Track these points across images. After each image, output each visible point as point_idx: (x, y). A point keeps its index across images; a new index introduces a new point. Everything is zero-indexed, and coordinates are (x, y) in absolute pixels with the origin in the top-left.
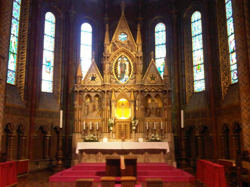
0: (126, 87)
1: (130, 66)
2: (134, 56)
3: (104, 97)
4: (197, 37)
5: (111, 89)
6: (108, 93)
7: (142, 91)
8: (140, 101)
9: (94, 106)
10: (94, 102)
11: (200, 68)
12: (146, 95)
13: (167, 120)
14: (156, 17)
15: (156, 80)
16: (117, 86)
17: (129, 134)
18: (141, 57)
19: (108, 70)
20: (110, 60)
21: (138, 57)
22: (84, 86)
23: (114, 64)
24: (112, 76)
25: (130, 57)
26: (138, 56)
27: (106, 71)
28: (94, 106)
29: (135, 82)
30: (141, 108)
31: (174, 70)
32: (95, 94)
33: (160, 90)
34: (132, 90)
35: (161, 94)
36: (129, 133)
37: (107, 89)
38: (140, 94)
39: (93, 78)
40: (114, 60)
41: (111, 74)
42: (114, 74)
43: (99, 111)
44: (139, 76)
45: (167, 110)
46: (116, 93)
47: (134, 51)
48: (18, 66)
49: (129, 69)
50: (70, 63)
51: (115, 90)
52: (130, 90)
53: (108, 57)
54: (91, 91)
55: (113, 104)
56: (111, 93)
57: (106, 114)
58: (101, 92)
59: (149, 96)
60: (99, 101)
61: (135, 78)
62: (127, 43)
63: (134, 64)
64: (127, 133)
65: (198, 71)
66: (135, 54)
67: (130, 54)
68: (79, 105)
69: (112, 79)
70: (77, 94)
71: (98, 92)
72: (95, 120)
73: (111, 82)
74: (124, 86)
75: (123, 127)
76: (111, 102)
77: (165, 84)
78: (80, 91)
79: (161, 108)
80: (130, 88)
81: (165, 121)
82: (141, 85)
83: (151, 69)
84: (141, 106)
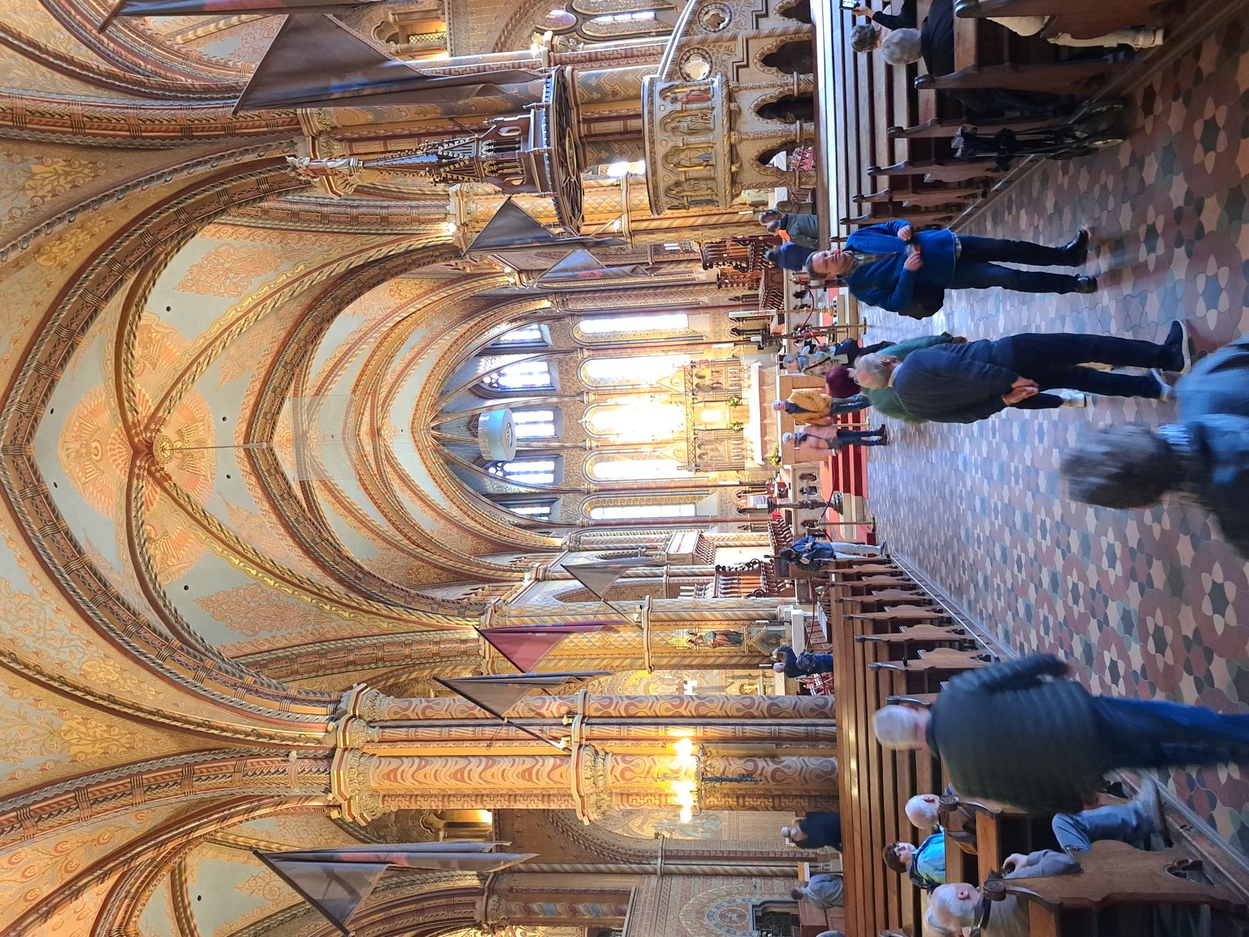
35: (695, 371)
50: (654, 486)
55: (709, 428)
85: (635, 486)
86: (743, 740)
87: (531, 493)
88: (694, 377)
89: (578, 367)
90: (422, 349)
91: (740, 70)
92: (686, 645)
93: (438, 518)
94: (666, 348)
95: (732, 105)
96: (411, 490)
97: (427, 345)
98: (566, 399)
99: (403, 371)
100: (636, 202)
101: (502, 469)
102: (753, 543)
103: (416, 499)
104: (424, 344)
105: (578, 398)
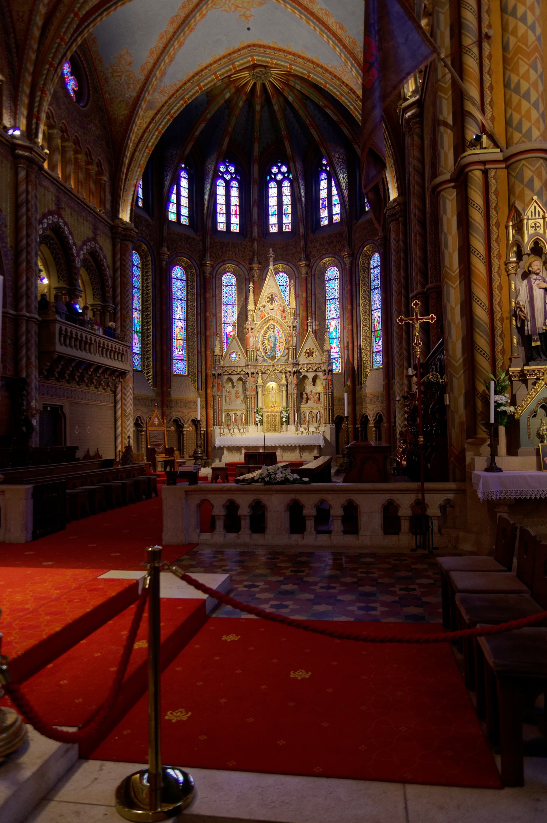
0: (275, 367)
4: (376, 291)
5: (257, 370)
7: (295, 372)
9: (237, 393)
10: (238, 387)
12: (301, 377)
22: (223, 367)
28: (237, 393)
29: (288, 359)
31: (348, 338)
32: (238, 376)
36: (280, 425)
38: (292, 375)
40: (260, 332)
46: (264, 375)
48: (144, 347)
50: (208, 333)
55: (260, 389)
56: (257, 375)
57: (251, 403)
61: (288, 354)
65: (377, 339)
76: (257, 387)
78: (219, 375)
80: (281, 369)
85: (208, 314)
87: (204, 205)
88: (314, 374)
89: (334, 254)
90: (340, 40)
93: (146, 72)
94: (350, 346)
96: (175, 33)
97: (345, 46)
98: (302, 243)
99: (312, 14)
100: (528, 174)
101: (232, 179)
102: (119, 430)
103: (164, 41)
104: (347, 42)
105: (303, 256)
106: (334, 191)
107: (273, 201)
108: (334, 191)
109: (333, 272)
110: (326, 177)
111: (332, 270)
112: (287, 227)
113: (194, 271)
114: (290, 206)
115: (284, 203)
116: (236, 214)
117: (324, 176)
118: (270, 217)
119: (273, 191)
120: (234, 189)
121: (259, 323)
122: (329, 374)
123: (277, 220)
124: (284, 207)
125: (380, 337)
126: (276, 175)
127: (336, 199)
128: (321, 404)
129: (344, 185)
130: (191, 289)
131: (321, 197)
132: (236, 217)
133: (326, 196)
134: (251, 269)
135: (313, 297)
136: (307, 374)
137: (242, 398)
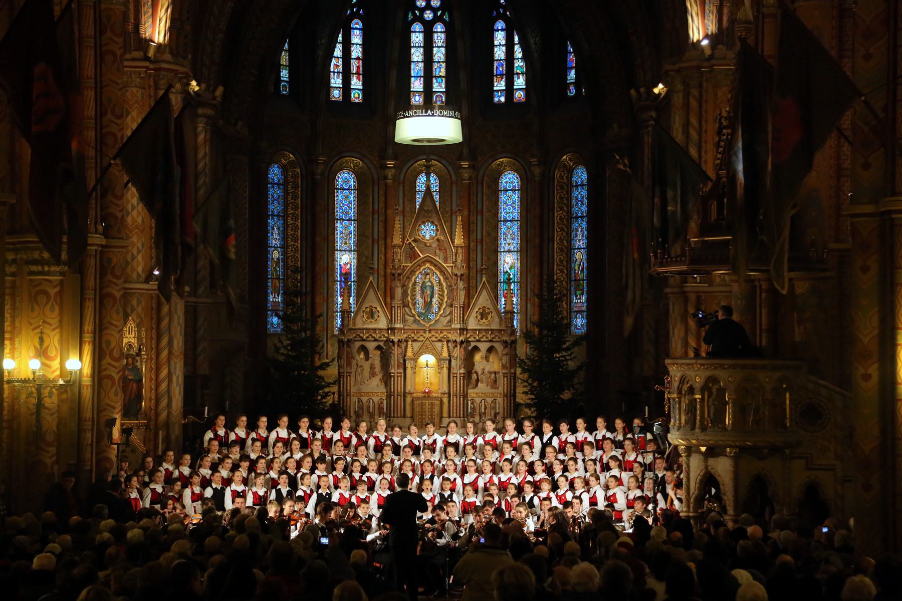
0: (433, 333)
1: (442, 290)
2: (449, 270)
3: (393, 352)
5: (405, 336)
6: (400, 344)
7: (462, 343)
8: (458, 360)
9: (372, 367)
11: (581, 288)
12: (470, 348)
13: (507, 396)
14: (501, 160)
15: (489, 318)
16: (417, 330)
17: (438, 420)
18: (462, 275)
19: (399, 299)
20: (403, 278)
21: (456, 275)
23: (410, 285)
24: (406, 309)
25: (441, 272)
26: (456, 271)
27: (397, 302)
28: (372, 367)
29: (451, 321)
30: (460, 374)
32: (375, 344)
33: (497, 339)
34: (444, 338)
35: (499, 347)
37: (399, 338)
38: (459, 346)
39: (371, 315)
41: (403, 307)
42: (410, 305)
43: (383, 376)
44: (457, 313)
45: (507, 376)
46: (415, 344)
47: (449, 259)
49: (439, 294)
51: (413, 337)
52: (442, 338)
53: (399, 275)
54: (369, 339)
55: (408, 365)
58: (386, 341)
59: (476, 349)
60: (381, 358)
61: (451, 313)
62: (434, 245)
63: (449, 286)
64: (435, 418)
65: (578, 293)
66: (452, 267)
67: (440, 266)
68: (347, 367)
69: (406, 316)
70: (343, 346)
71: (382, 341)
72: (376, 393)
73: (404, 321)
74: (430, 331)
75: (427, 405)
76: (405, 361)
77: (505, 328)
78: (349, 341)
79: (499, 372)
80: (442, 335)
81: (504, 396)
82: (460, 329)
83: (481, 297)
84: (460, 369)
85: (318, 239)
86: (80, 431)
91: (803, 461)
92: (125, 341)
95: (766, 451)
106: (518, 53)
107: (417, 55)
108: (518, 53)
109: (510, 180)
110: (504, 27)
111: (510, 176)
112: (439, 99)
113: (298, 170)
114: (444, 65)
115: (436, 59)
116: (358, 73)
117: (500, 24)
118: (413, 79)
119: (417, 38)
120: (357, 32)
121: (411, 265)
122: (511, 347)
123: (422, 86)
124: (435, 66)
125: (582, 290)
126: (422, 10)
127: (519, 65)
128: (497, 388)
129: (536, 54)
130: (292, 198)
131: (497, 57)
132: (358, 79)
133: (503, 56)
134: (384, 167)
135: (479, 217)
136: (478, 344)
137: (380, 376)
